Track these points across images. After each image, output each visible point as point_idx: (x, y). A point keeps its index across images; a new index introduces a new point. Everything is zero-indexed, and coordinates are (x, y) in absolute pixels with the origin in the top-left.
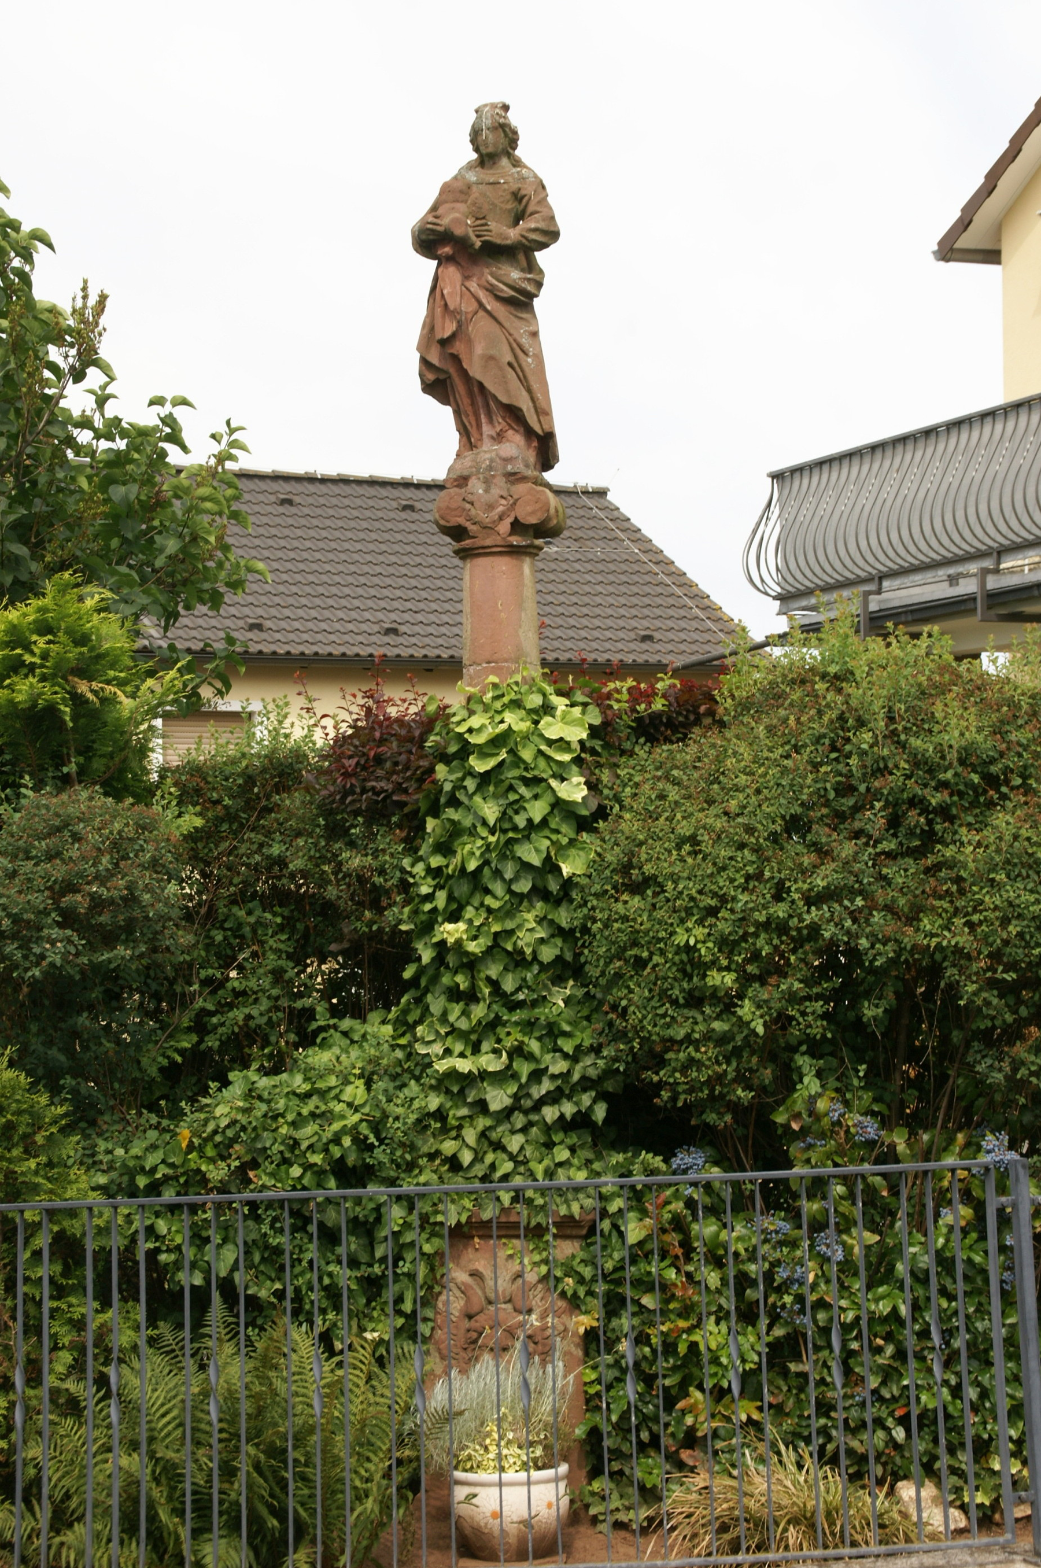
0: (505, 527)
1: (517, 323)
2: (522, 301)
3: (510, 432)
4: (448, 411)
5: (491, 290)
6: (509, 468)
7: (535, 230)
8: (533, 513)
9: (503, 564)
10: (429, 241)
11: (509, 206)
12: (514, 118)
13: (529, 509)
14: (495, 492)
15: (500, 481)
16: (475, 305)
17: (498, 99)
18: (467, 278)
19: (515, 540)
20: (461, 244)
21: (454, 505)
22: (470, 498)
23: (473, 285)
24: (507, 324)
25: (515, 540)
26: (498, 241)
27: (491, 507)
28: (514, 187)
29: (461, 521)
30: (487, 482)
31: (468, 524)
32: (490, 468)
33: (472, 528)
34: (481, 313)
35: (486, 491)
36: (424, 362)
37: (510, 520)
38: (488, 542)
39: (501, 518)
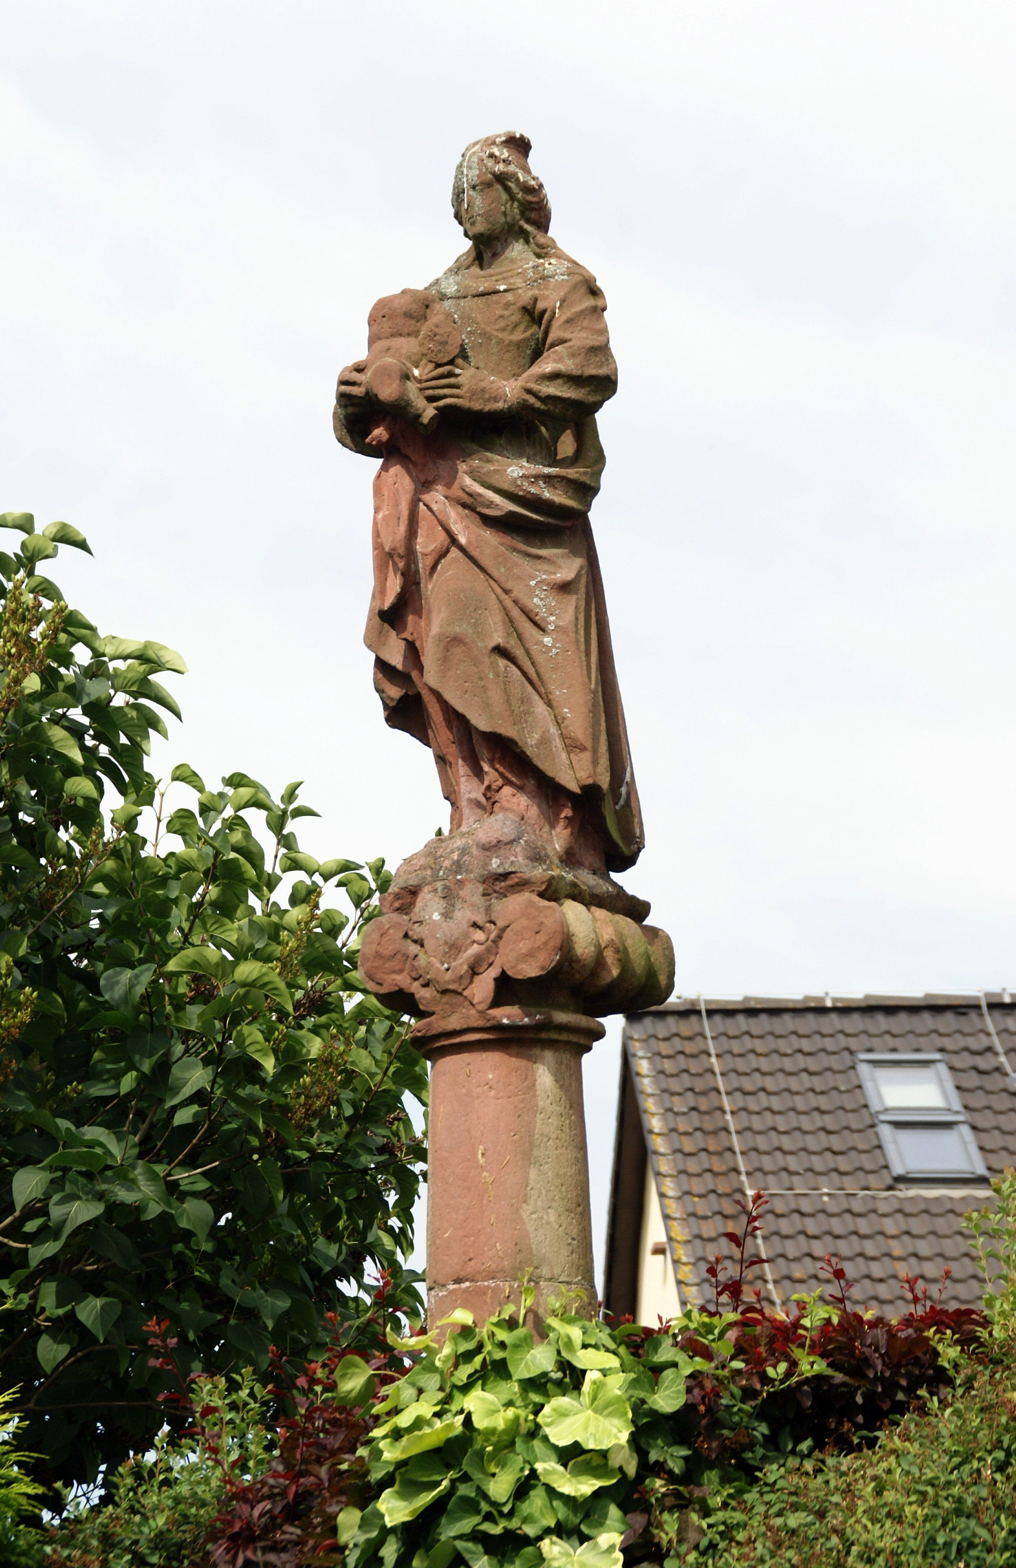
0: (483, 988)
1: (525, 564)
2: (558, 524)
3: (507, 790)
4: (427, 754)
5: (469, 504)
6: (495, 863)
7: (554, 376)
8: (530, 954)
9: (489, 1068)
10: (363, 418)
11: (518, 336)
12: (541, 166)
13: (524, 947)
14: (464, 915)
15: (472, 893)
16: (442, 536)
17: (500, 129)
18: (424, 485)
19: (507, 1015)
20: (397, 413)
21: (388, 949)
22: (417, 931)
23: (436, 498)
24: (499, 572)
25: (507, 1015)
26: (477, 406)
27: (454, 948)
28: (525, 296)
29: (402, 980)
30: (449, 896)
31: (415, 988)
32: (458, 867)
33: (424, 995)
34: (454, 553)
35: (447, 915)
36: (381, 665)
37: (493, 973)
38: (454, 1022)
39: (474, 971)
